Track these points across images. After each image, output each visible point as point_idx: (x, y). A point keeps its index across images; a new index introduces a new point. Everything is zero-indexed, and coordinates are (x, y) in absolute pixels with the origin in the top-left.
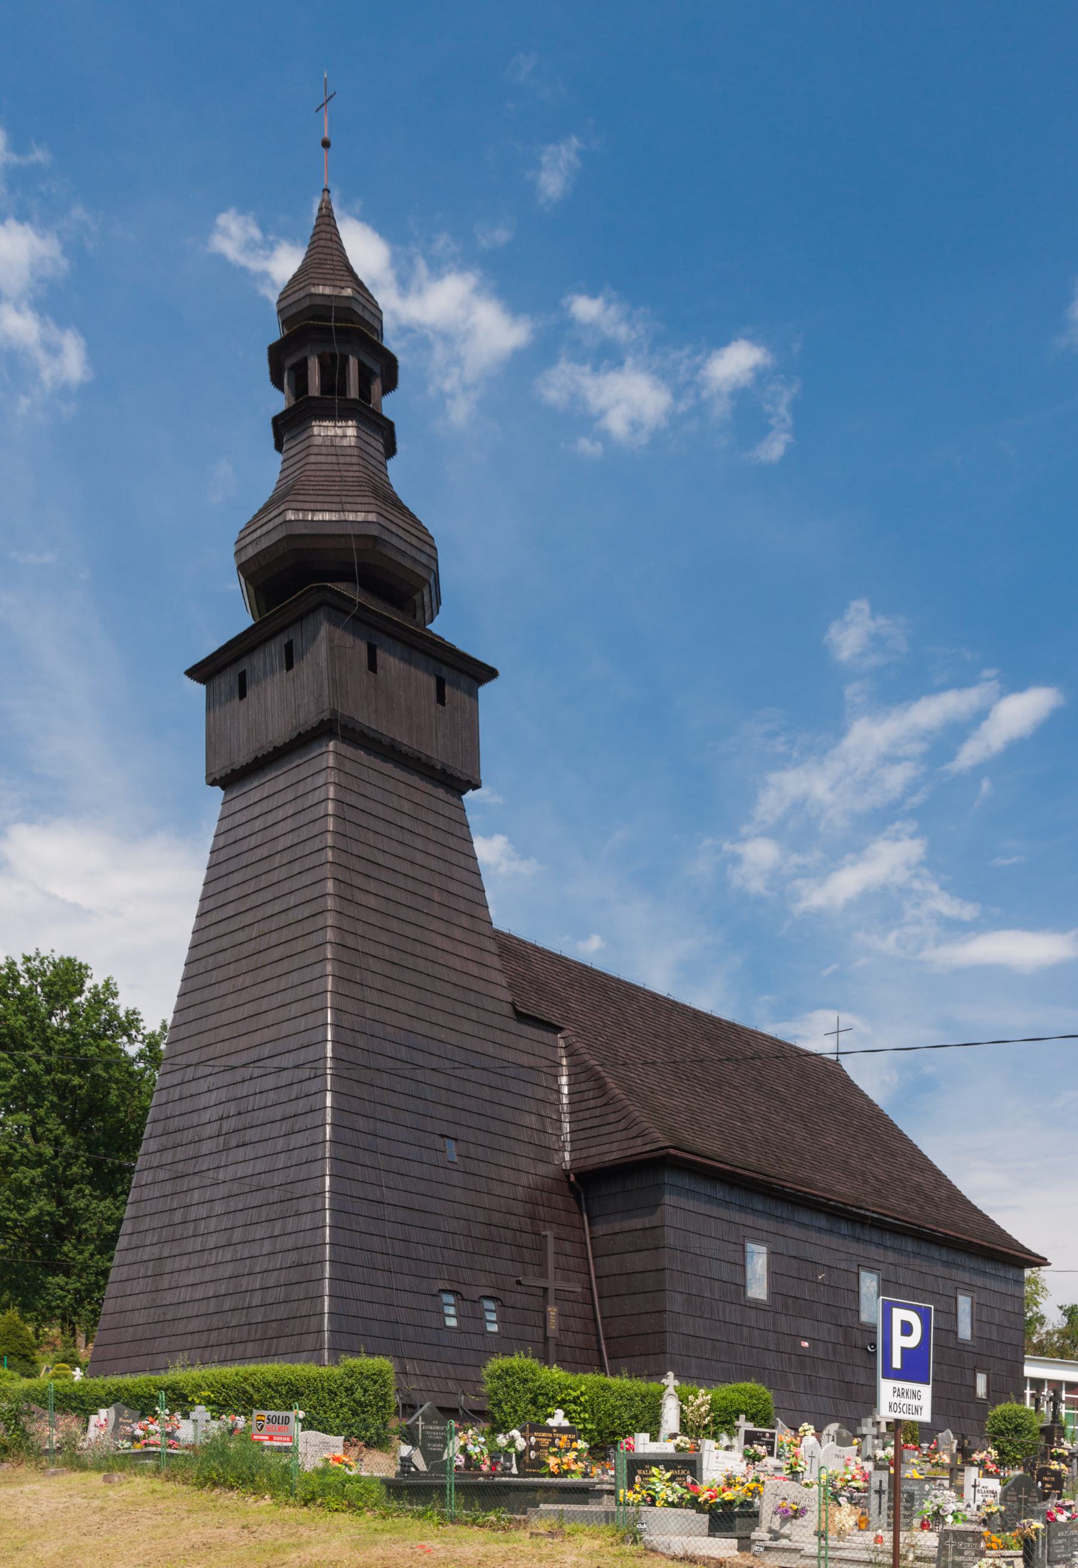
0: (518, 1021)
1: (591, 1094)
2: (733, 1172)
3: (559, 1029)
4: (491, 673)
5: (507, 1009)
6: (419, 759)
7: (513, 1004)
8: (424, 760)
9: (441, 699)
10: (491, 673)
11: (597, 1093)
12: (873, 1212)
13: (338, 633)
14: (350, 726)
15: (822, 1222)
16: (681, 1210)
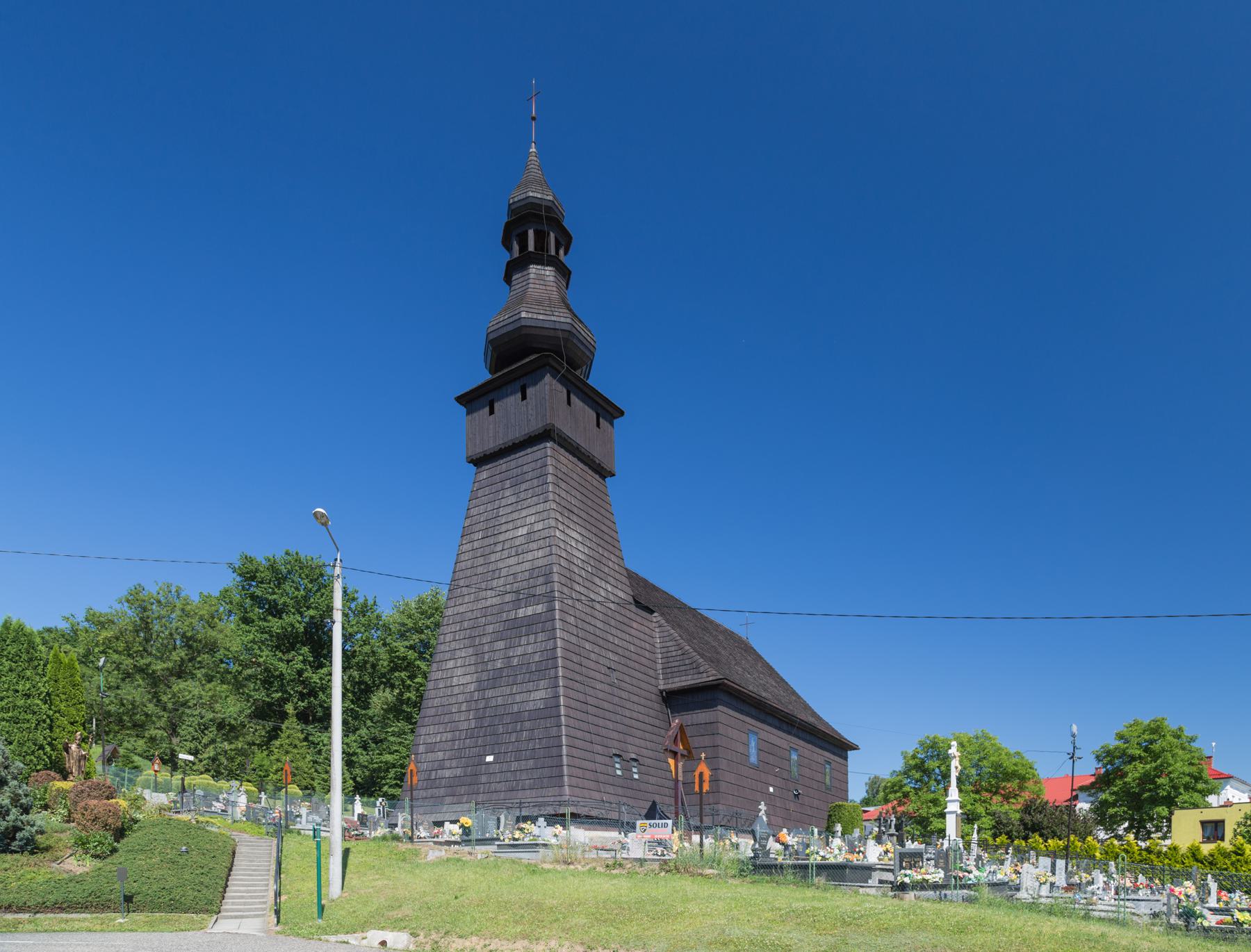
3: (652, 612)
4: (622, 413)
5: (631, 600)
10: (622, 413)
13: (554, 382)
15: (776, 722)
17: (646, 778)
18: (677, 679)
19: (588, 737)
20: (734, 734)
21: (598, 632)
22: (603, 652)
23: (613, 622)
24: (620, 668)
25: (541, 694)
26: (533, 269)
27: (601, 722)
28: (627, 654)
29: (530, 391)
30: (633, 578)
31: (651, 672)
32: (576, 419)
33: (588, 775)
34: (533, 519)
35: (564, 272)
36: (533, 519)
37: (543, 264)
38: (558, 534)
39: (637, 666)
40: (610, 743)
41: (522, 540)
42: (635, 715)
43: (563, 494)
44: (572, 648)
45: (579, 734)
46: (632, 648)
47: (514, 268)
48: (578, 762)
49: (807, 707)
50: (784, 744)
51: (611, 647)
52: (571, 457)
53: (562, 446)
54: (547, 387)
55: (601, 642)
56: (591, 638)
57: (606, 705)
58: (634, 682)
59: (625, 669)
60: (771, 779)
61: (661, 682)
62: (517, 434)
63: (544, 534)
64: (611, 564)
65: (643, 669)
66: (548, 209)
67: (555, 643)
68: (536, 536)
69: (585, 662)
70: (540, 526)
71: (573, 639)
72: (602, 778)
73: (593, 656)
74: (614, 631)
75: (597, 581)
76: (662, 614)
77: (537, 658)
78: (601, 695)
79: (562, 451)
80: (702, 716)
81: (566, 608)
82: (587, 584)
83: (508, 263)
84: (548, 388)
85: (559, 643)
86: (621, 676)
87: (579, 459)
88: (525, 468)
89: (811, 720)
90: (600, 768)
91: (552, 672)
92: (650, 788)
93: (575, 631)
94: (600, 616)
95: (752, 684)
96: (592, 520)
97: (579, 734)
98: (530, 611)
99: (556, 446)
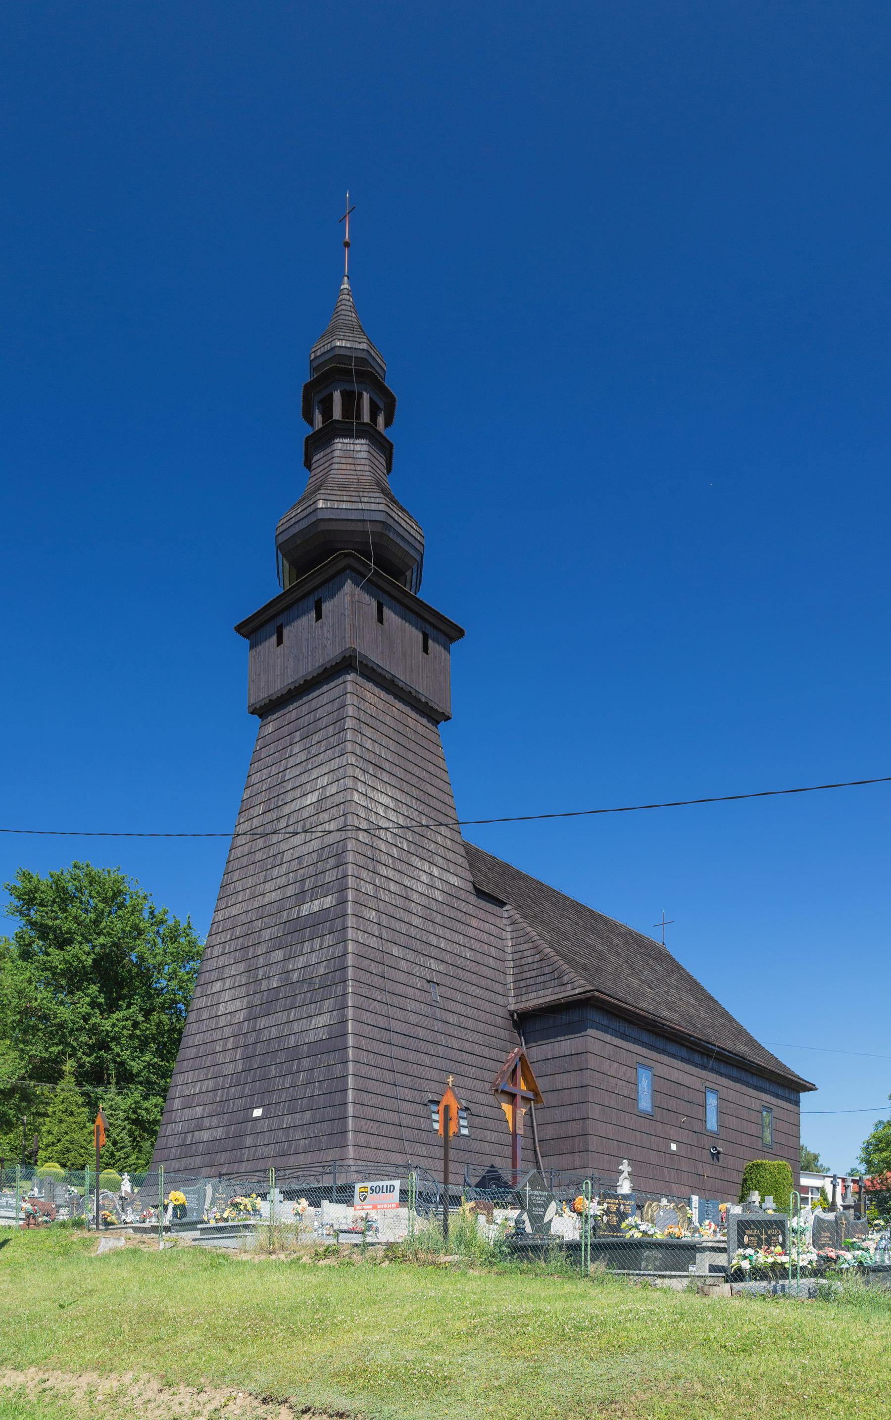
0: (478, 897)
1: (528, 953)
2: (634, 1012)
3: (502, 904)
4: (461, 633)
6: (411, 693)
7: (473, 883)
8: (414, 694)
9: (426, 649)
10: (461, 633)
11: (533, 951)
12: (718, 1047)
14: (365, 662)
15: (683, 1052)
16: (597, 1042)
17: (480, 1134)
18: (533, 995)
19: (389, 1076)
20: (615, 1069)
21: (414, 932)
22: (421, 959)
23: (438, 918)
24: (447, 981)
25: (323, 1020)
26: (340, 444)
27: (412, 1056)
28: (459, 961)
29: (326, 607)
30: (473, 856)
31: (498, 988)
32: (395, 643)
33: (386, 1129)
34: (325, 780)
35: (384, 447)
36: (325, 780)
37: (351, 437)
38: (356, 797)
39: (475, 979)
40: (424, 1085)
41: (311, 810)
42: (467, 1046)
43: (369, 744)
44: (370, 953)
45: (374, 1073)
46: (468, 954)
47: (317, 443)
48: (369, 1112)
49: (740, 1032)
50: (697, 1084)
51: (434, 952)
52: (383, 694)
53: (369, 679)
54: (348, 598)
55: (418, 945)
56: (403, 940)
57: (421, 1033)
58: (469, 1000)
59: (456, 983)
60: (674, 1132)
61: (511, 1000)
62: (308, 668)
63: (339, 798)
64: (439, 839)
65: (483, 982)
66: (362, 361)
67: (346, 948)
68: (328, 803)
69: (389, 973)
70: (333, 789)
71: (373, 942)
72: (407, 1133)
73: (403, 965)
74: (440, 931)
75: (417, 862)
76: (518, 907)
77: (322, 970)
78: (413, 1018)
79: (370, 686)
80: (566, 1045)
81: (363, 899)
82: (399, 866)
83: (307, 439)
84: (350, 602)
85: (351, 947)
86: (449, 993)
87: (397, 697)
88: (319, 714)
89: (741, 1048)
90: (406, 1120)
91: (340, 988)
92: (487, 1148)
93: (376, 930)
94: (420, 910)
95: (649, 1001)
96: (414, 781)
97: (374, 1073)
98: (316, 906)
99: (360, 680)
